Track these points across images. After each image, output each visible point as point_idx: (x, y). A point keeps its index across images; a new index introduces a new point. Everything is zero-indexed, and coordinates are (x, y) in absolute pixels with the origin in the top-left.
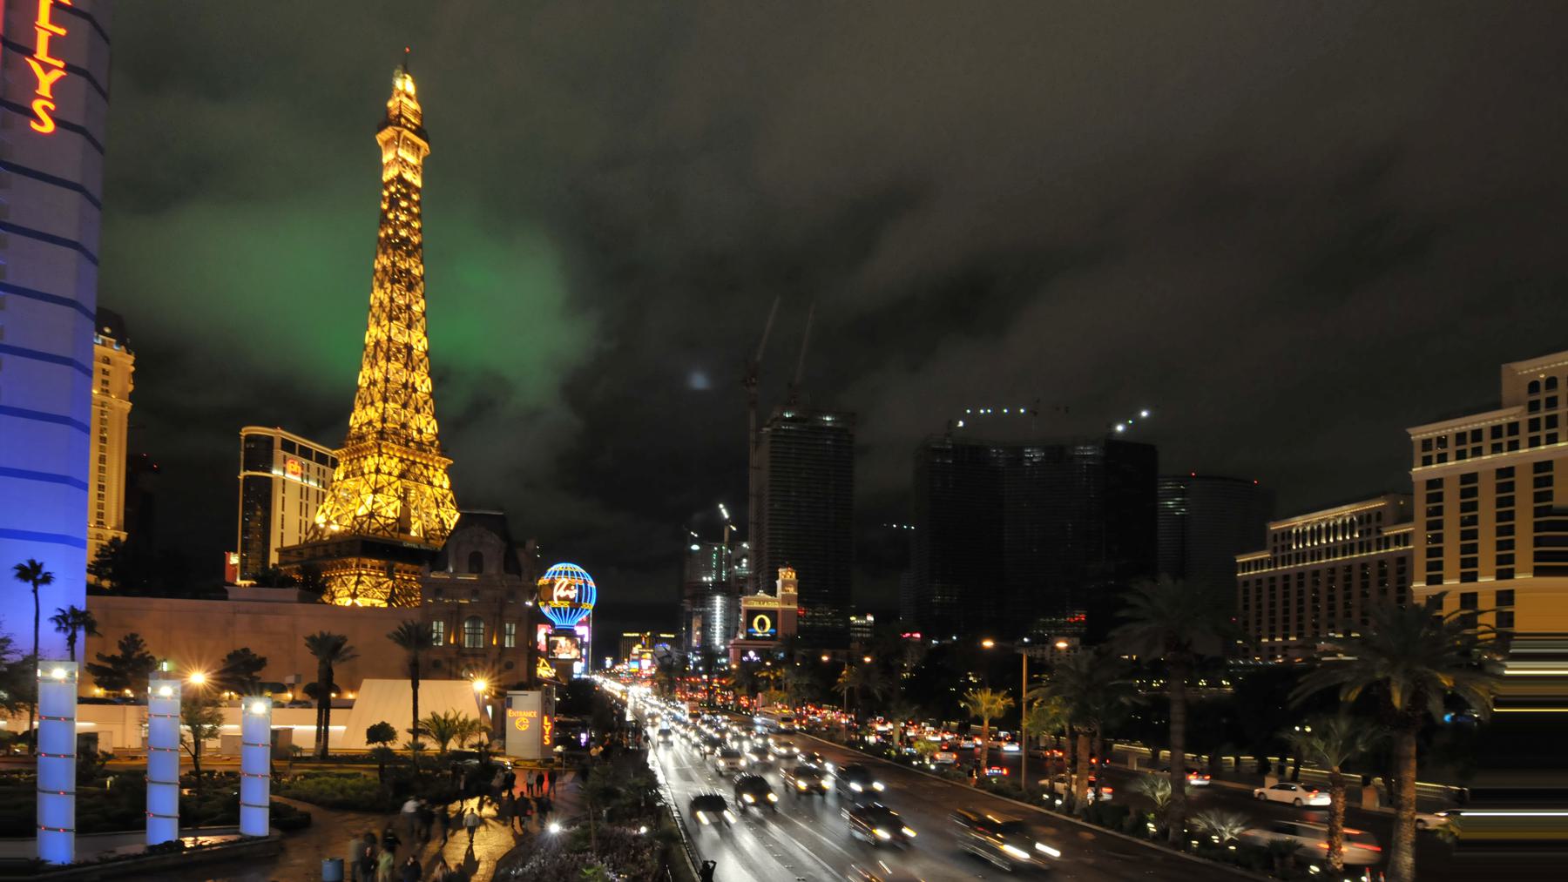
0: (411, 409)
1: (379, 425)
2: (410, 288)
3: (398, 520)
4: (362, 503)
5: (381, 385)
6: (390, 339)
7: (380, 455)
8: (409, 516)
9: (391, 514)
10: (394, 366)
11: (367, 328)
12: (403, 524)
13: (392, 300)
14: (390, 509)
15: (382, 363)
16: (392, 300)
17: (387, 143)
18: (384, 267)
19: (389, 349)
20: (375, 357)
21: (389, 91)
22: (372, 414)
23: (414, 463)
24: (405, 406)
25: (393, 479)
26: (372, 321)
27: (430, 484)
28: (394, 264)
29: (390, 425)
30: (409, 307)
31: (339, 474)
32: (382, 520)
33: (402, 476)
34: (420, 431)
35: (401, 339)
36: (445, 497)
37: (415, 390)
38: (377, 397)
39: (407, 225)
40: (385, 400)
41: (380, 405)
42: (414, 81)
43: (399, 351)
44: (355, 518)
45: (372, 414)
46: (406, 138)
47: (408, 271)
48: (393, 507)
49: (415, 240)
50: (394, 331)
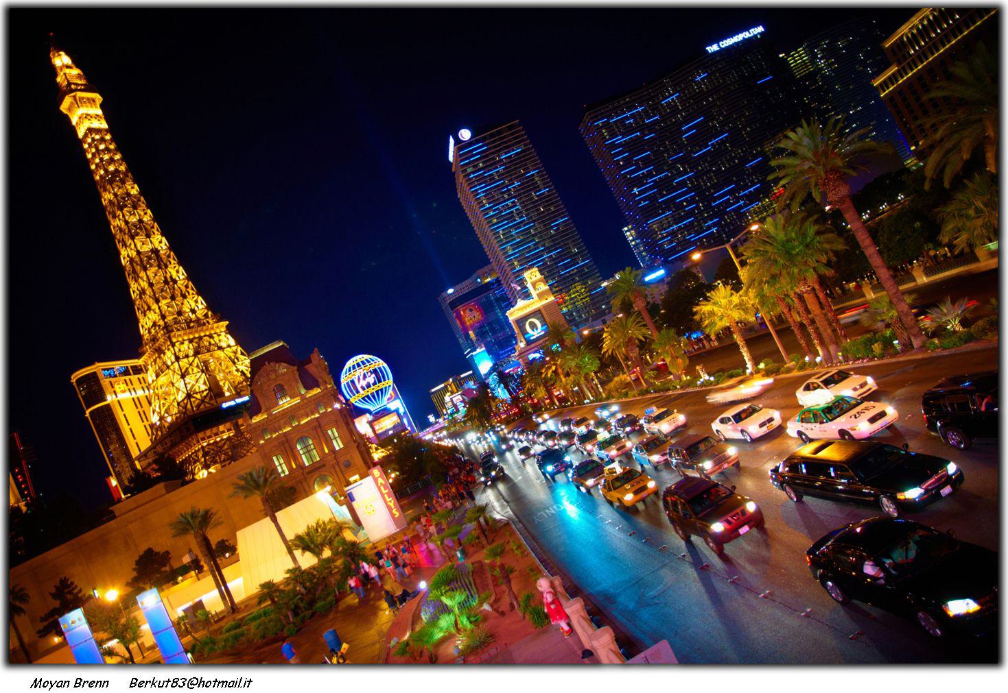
0: (179, 298)
1: (161, 323)
2: (135, 207)
3: (210, 389)
4: (178, 390)
5: (149, 292)
6: (139, 253)
7: (173, 345)
8: (217, 383)
9: (203, 388)
10: (151, 272)
11: (119, 254)
12: (215, 391)
13: (127, 222)
14: (200, 384)
15: (142, 274)
16: (127, 222)
17: (69, 109)
18: (110, 201)
19: (141, 259)
20: (134, 271)
21: (53, 71)
22: (154, 316)
23: (200, 338)
24: (173, 298)
25: (191, 359)
26: (120, 246)
27: (220, 348)
28: (116, 195)
29: (169, 319)
30: (141, 221)
31: (150, 376)
32: (198, 396)
33: (197, 353)
34: (193, 311)
35: (146, 248)
36: (235, 353)
37: (175, 282)
38: (151, 301)
39: (112, 160)
40: (157, 301)
41: (155, 306)
42: (68, 54)
43: (150, 258)
44: (178, 404)
45: (154, 316)
46: (83, 98)
47: (128, 194)
48: (201, 381)
49: (122, 168)
50: (139, 245)
